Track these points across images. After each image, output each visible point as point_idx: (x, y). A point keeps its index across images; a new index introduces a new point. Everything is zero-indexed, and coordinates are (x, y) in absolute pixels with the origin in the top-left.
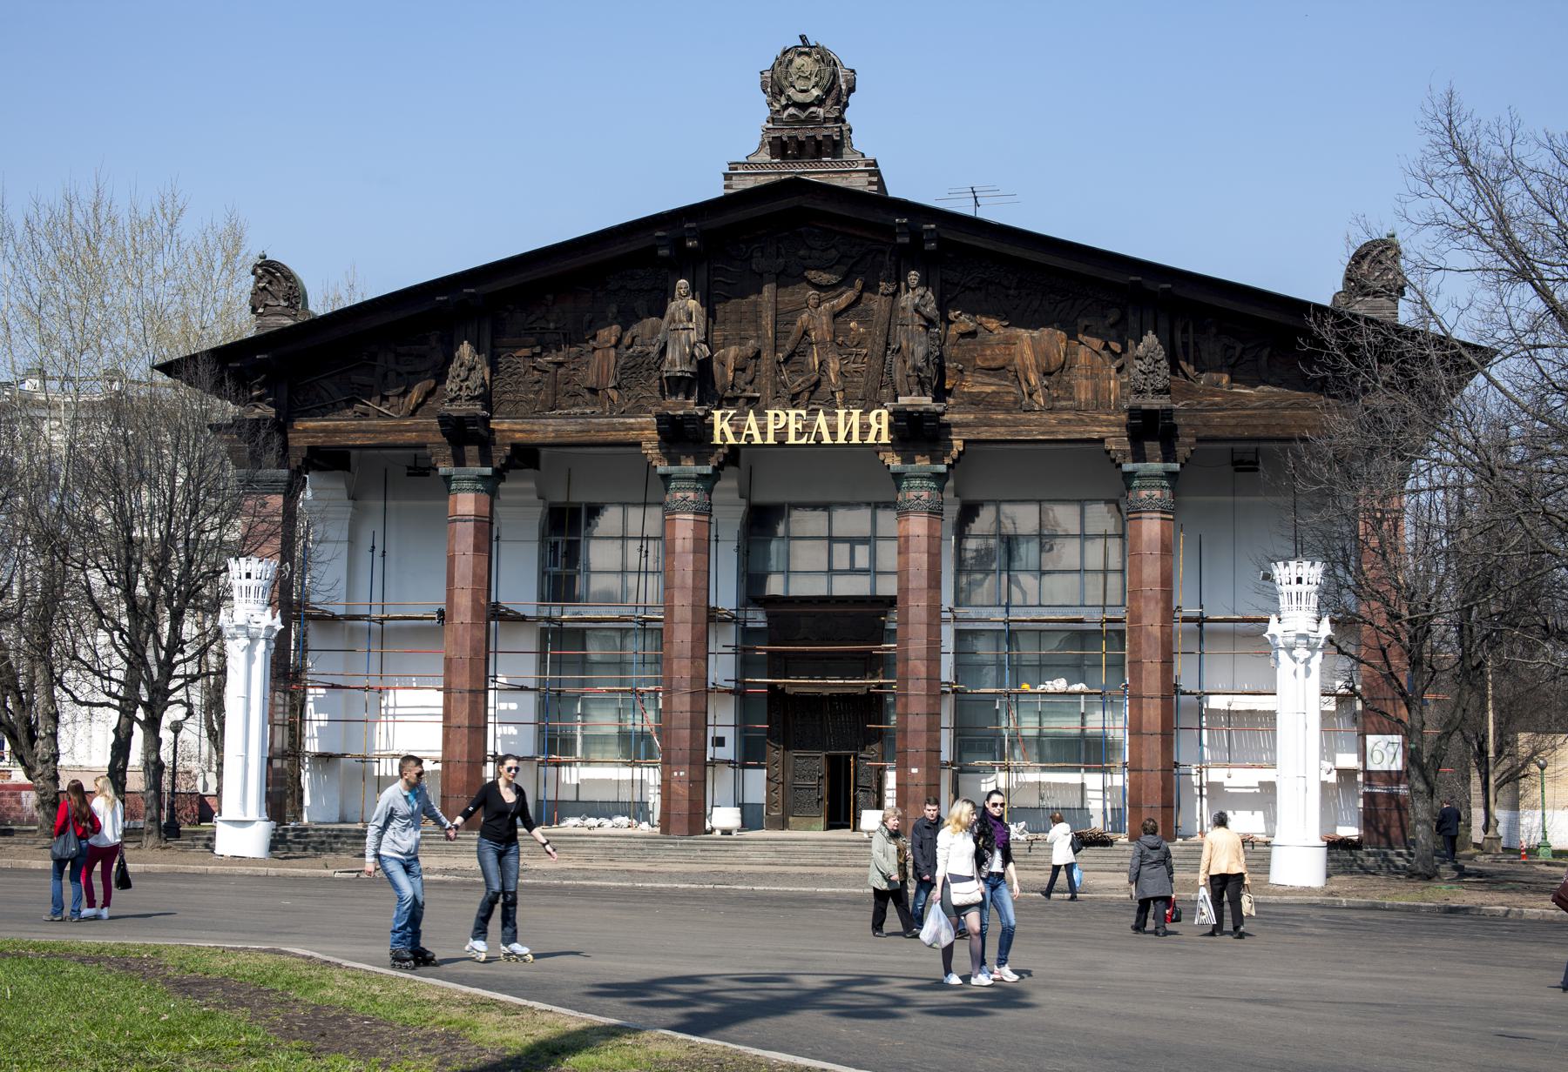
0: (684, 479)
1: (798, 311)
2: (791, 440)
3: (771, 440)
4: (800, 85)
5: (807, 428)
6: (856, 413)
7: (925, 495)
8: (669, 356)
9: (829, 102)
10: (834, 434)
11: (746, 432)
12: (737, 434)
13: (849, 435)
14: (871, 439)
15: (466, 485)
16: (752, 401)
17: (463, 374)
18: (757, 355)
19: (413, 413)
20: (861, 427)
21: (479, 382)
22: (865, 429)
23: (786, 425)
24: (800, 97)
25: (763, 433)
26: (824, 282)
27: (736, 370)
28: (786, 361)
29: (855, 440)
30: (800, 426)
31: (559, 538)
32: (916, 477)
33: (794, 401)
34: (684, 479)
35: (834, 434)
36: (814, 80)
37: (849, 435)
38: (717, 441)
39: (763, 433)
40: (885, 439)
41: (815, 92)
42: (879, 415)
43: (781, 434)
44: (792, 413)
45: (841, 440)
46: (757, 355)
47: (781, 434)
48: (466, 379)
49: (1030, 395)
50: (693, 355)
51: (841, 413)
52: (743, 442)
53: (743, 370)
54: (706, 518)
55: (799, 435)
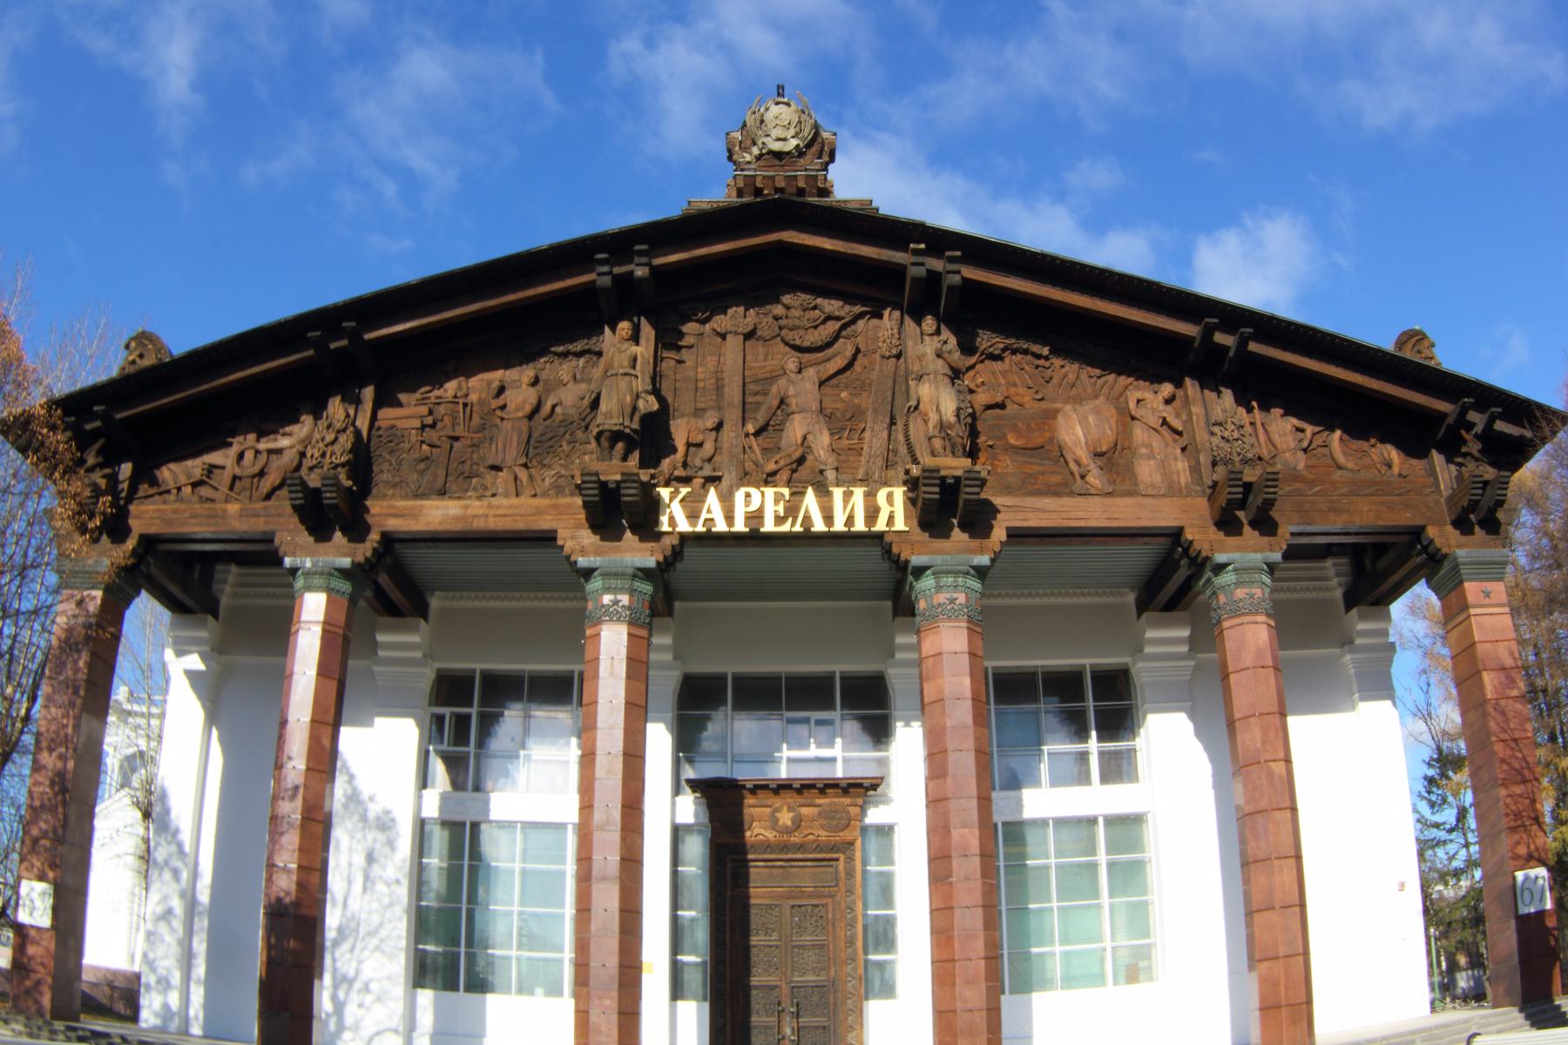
0: (616, 575)
1: (773, 378)
2: (769, 526)
3: (740, 526)
4: (775, 133)
5: (792, 511)
6: (859, 493)
7: (961, 598)
8: (603, 407)
9: (809, 156)
10: (828, 518)
11: (704, 515)
12: (693, 516)
13: (850, 520)
14: (881, 526)
15: (317, 581)
16: (713, 480)
17: (330, 437)
18: (718, 427)
19: (268, 497)
20: (867, 510)
21: (349, 445)
22: (872, 514)
23: (761, 510)
24: (777, 146)
25: (730, 519)
26: (806, 344)
27: (689, 445)
28: (757, 434)
29: (860, 526)
30: (781, 509)
31: (446, 711)
32: (948, 573)
33: (769, 479)
34: (616, 575)
35: (828, 518)
36: (792, 132)
37: (850, 520)
38: (665, 527)
39: (730, 519)
40: (900, 525)
41: (794, 142)
42: (890, 496)
43: (756, 517)
44: (770, 492)
45: (839, 526)
46: (718, 427)
47: (756, 517)
48: (333, 443)
49: (1083, 477)
50: (635, 409)
51: (838, 493)
52: (700, 528)
53: (700, 445)
54: (644, 633)
55: (779, 520)
